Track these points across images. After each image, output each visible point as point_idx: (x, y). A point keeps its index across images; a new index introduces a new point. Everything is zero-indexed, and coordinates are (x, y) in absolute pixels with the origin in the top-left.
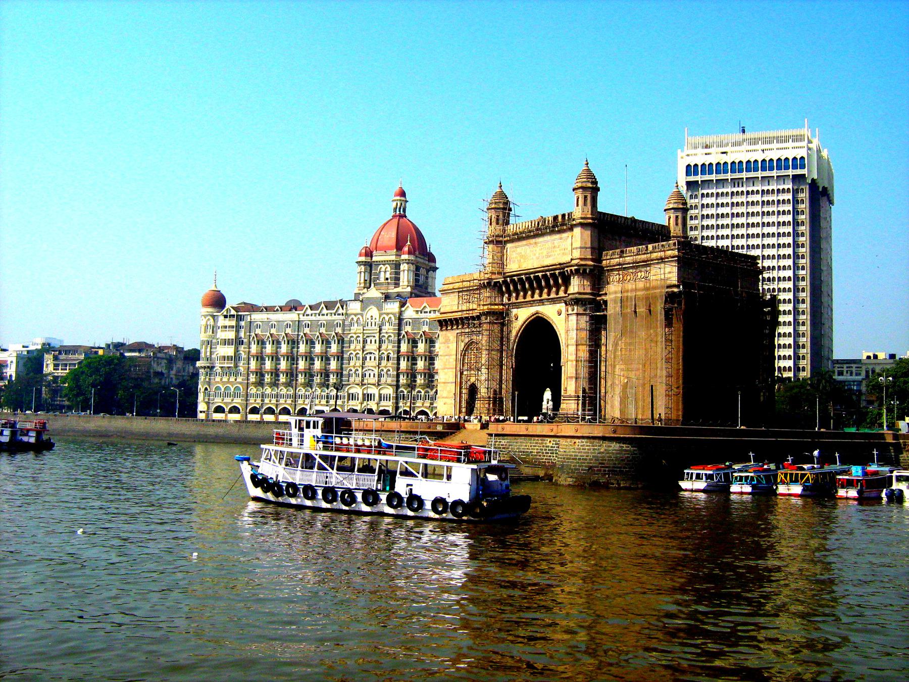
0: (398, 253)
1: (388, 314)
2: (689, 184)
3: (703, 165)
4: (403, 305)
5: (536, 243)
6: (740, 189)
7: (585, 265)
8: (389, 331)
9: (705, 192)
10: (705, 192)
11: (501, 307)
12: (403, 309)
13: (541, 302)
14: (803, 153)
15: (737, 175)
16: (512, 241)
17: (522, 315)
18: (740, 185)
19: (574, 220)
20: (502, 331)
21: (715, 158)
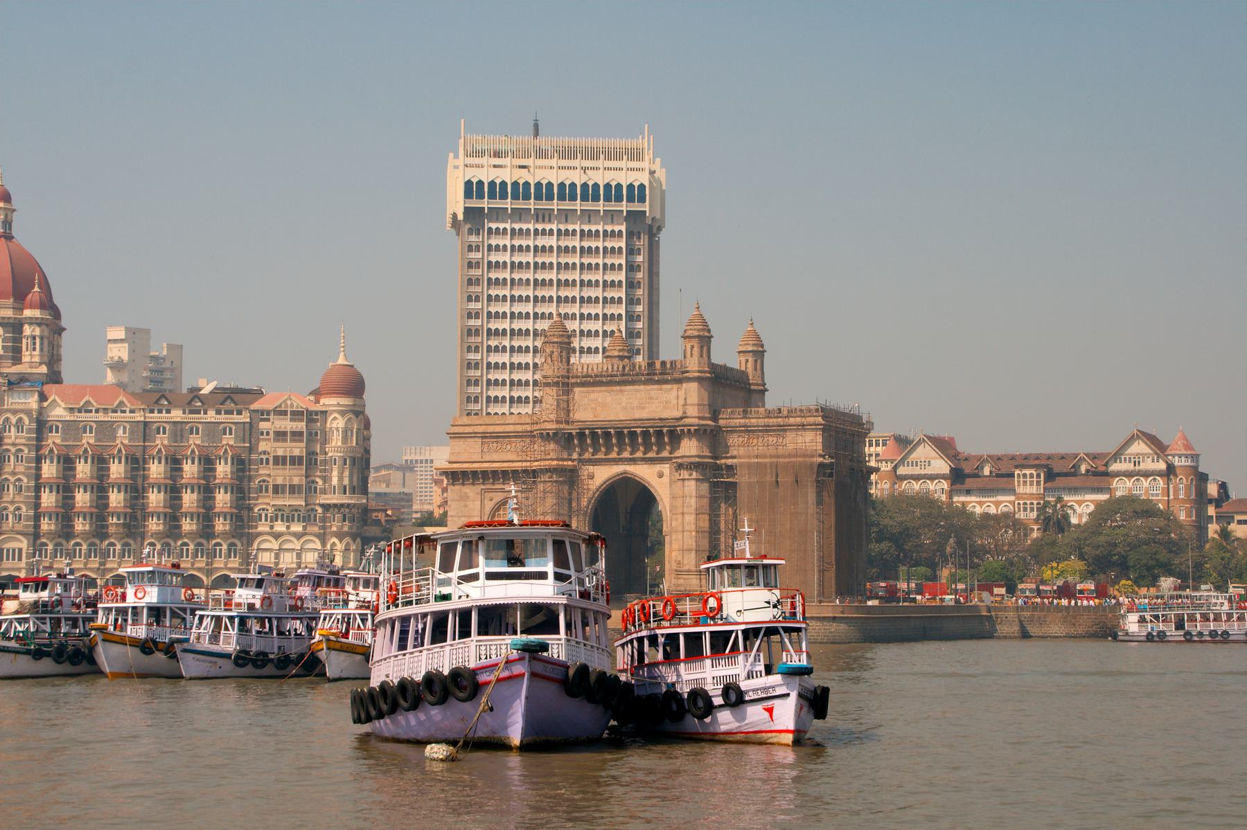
0: (17, 305)
1: (15, 412)
2: (468, 211)
3: (492, 184)
4: (43, 397)
5: (621, 391)
6: (548, 227)
7: (707, 425)
8: (18, 441)
9: (494, 226)
10: (494, 226)
11: (570, 463)
12: (45, 404)
13: (633, 461)
14: (644, 179)
15: (544, 205)
16: (583, 385)
17: (600, 475)
18: (547, 219)
19: (688, 372)
20: (570, 494)
21: (507, 175)
